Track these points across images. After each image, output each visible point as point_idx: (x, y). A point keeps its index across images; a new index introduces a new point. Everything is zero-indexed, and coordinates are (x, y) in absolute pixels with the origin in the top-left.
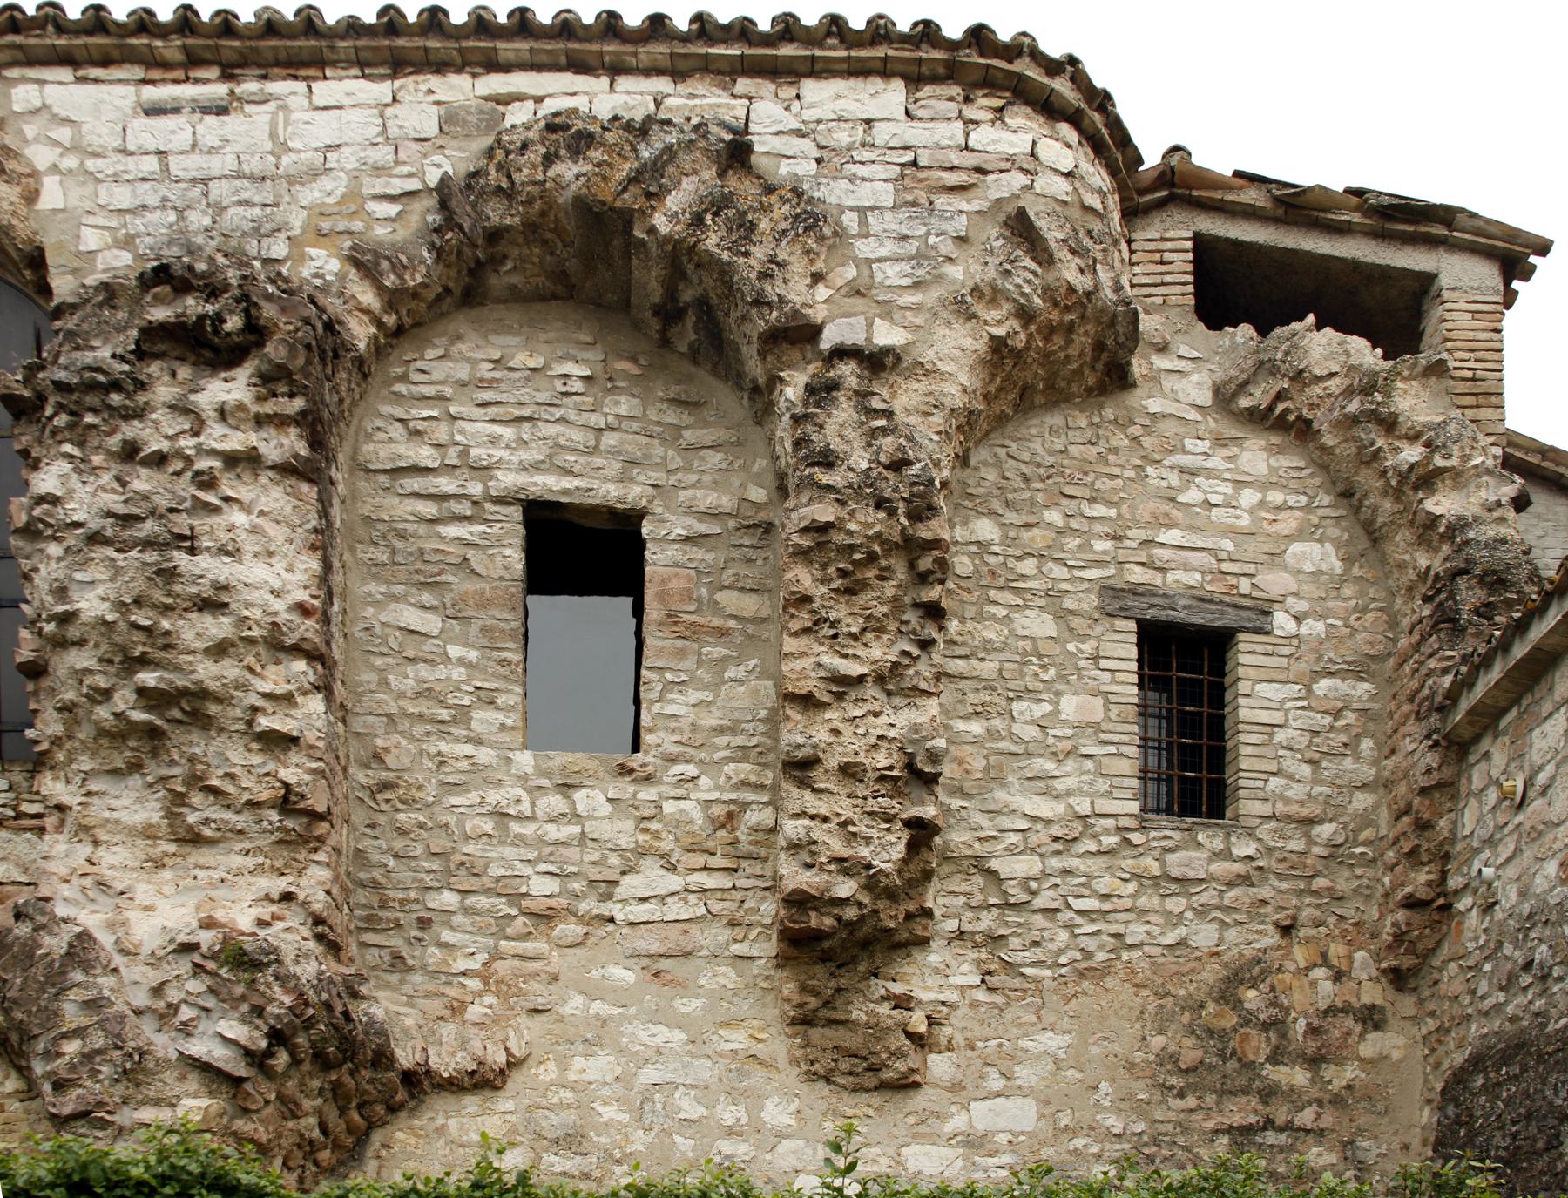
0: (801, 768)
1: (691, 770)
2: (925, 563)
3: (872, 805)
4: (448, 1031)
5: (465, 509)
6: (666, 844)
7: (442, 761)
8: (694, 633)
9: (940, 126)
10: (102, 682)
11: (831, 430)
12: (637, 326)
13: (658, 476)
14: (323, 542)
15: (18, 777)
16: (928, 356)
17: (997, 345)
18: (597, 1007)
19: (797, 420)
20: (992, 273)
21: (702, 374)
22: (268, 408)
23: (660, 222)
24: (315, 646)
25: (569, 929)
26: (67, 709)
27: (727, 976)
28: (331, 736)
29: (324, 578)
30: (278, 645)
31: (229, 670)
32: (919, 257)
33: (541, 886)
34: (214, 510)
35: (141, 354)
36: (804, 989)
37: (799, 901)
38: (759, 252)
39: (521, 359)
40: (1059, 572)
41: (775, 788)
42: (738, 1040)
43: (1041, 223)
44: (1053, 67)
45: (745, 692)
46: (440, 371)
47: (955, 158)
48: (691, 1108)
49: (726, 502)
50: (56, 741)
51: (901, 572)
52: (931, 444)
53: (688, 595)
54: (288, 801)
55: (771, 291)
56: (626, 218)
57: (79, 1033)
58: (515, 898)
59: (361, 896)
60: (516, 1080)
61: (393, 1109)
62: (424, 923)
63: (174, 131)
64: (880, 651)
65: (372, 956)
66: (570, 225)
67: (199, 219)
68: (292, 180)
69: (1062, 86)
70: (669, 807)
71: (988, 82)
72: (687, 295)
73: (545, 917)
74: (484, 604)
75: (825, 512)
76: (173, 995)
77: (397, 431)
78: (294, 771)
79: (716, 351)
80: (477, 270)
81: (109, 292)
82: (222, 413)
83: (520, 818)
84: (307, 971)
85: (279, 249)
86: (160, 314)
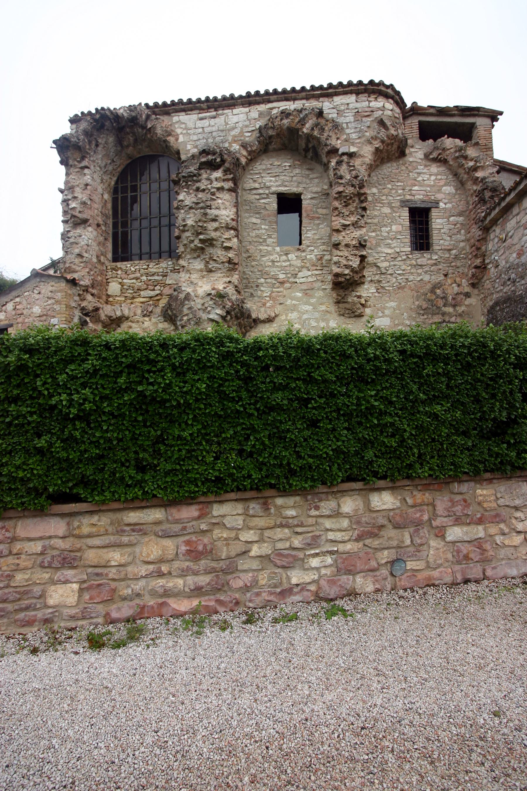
0: (336, 246)
1: (312, 248)
2: (363, 198)
3: (352, 253)
4: (262, 309)
5: (265, 196)
6: (308, 265)
7: (261, 251)
8: (313, 218)
9: (363, 103)
10: (192, 239)
11: (342, 171)
12: (300, 154)
13: (304, 185)
14: (236, 205)
15: (174, 261)
16: (362, 153)
17: (377, 149)
18: (294, 302)
19: (334, 170)
20: (375, 133)
21: (313, 163)
22: (226, 177)
23: (305, 130)
24: (235, 227)
25: (287, 285)
26: (185, 245)
27: (321, 293)
28: (238, 247)
29: (237, 213)
30: (228, 228)
31: (218, 234)
32: (360, 131)
33: (282, 276)
34: (214, 200)
35: (200, 169)
36: (338, 295)
37: (337, 275)
38: (325, 134)
39: (276, 163)
40: (391, 198)
41: (331, 251)
42: (323, 308)
43: (386, 121)
44: (387, 87)
45: (324, 230)
46: (259, 167)
47: (367, 109)
48: (314, 324)
49: (319, 190)
50: (183, 252)
51: (357, 201)
52: (363, 172)
53: (311, 210)
54: (230, 261)
55: (328, 142)
56: (298, 130)
57: (187, 315)
58: (276, 279)
59: (244, 281)
60: (277, 319)
61: (251, 328)
62: (257, 286)
63: (206, 123)
64: (353, 219)
65: (247, 294)
66: (286, 133)
67: (210, 140)
68: (229, 130)
69: (390, 91)
70: (308, 257)
71: (373, 92)
72: (310, 146)
73: (282, 283)
74: (269, 216)
75: (341, 189)
76: (206, 305)
77: (251, 181)
78: (231, 254)
79: (316, 157)
80: (267, 145)
81: (193, 157)
82: (216, 179)
83: (277, 262)
84: (234, 298)
85: (227, 145)
86: (203, 160)
